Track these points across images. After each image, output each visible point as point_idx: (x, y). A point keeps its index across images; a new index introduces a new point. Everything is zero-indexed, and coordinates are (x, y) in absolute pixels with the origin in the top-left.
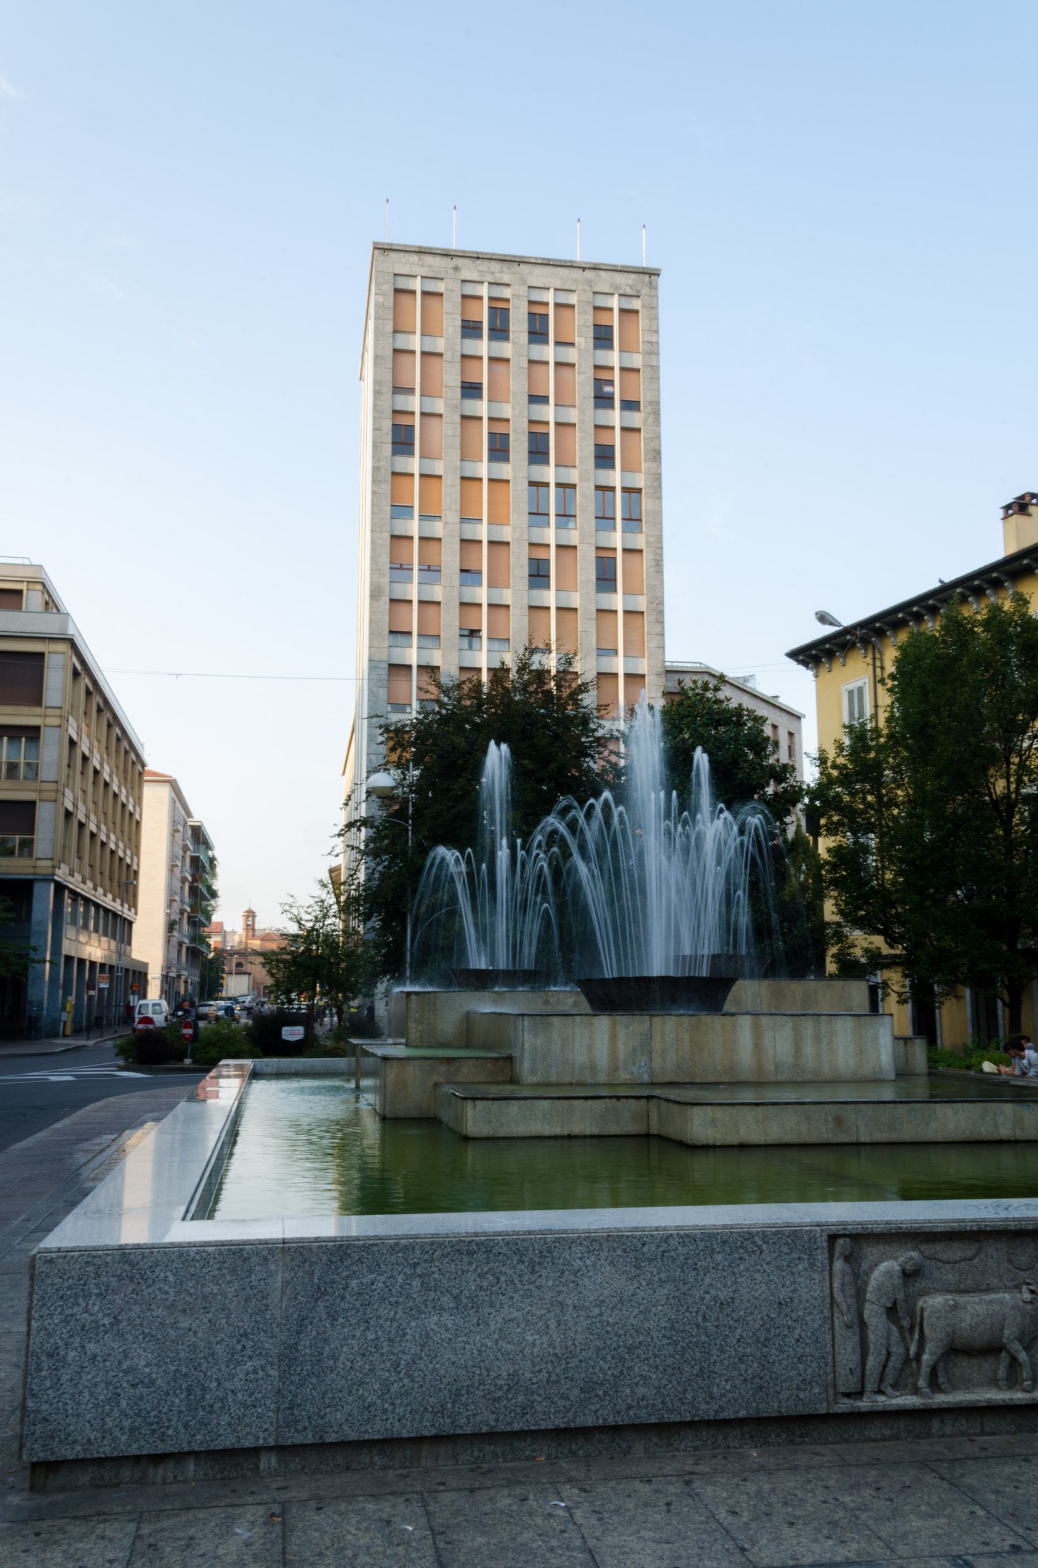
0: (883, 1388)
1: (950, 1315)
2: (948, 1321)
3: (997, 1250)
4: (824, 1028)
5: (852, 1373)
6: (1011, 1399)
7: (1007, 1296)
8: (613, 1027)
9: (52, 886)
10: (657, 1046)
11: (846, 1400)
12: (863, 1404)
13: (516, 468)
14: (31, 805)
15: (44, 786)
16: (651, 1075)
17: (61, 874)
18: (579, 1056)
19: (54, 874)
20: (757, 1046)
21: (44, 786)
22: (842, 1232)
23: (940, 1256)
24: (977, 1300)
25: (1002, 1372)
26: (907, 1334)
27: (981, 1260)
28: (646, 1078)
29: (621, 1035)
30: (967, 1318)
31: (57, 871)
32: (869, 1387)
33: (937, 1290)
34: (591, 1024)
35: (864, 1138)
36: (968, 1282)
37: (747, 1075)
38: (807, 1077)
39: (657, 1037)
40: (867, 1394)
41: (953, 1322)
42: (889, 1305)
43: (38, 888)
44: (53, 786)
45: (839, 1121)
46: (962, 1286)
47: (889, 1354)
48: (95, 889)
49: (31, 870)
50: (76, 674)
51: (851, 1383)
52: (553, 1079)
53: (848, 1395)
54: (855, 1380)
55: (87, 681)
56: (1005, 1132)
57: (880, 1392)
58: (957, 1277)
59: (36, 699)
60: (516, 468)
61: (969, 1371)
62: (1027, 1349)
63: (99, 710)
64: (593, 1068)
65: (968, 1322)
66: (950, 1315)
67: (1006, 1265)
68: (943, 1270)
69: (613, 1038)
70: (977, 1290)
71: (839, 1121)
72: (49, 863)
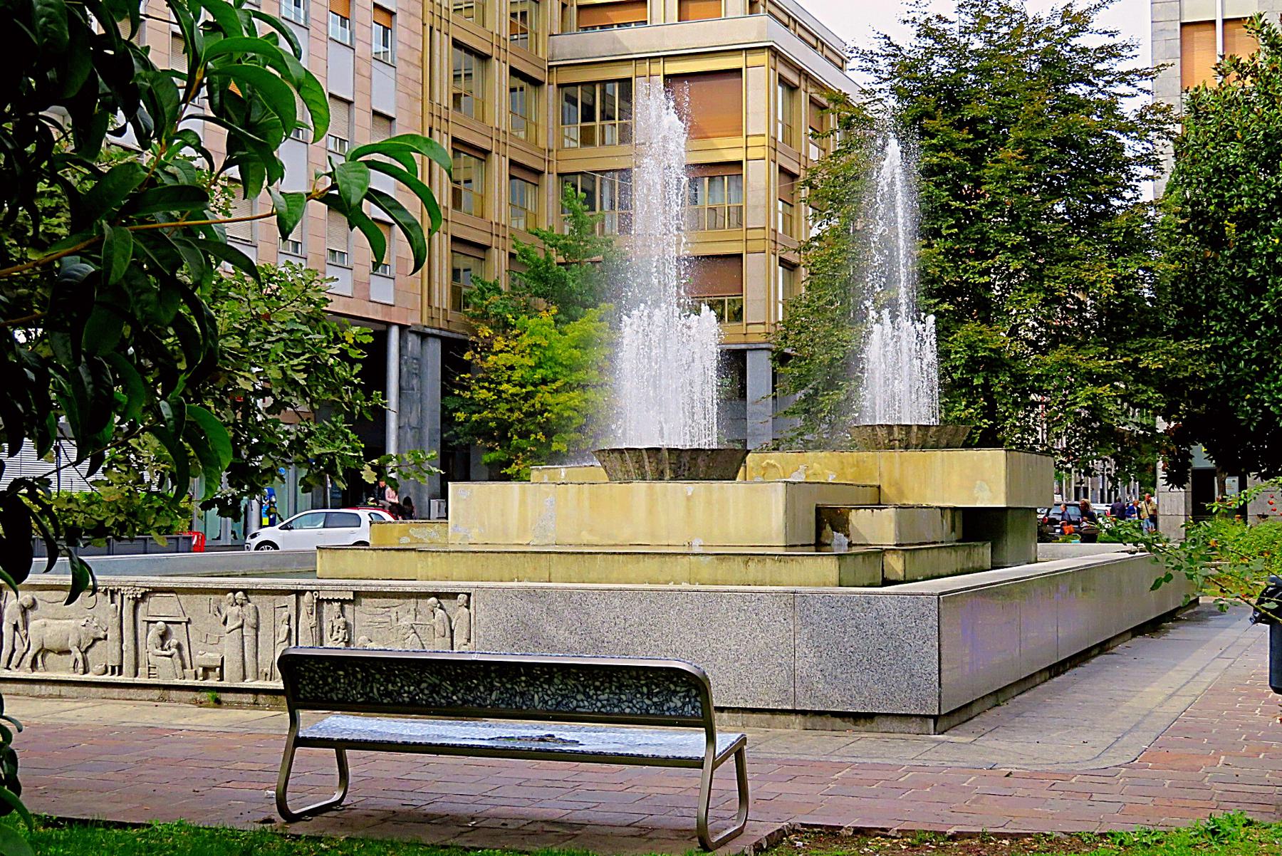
14: (740, 256)
15: (751, 234)
21: (751, 234)
47: (14, 650)
49: (742, 339)
50: (791, 89)
59: (738, 131)
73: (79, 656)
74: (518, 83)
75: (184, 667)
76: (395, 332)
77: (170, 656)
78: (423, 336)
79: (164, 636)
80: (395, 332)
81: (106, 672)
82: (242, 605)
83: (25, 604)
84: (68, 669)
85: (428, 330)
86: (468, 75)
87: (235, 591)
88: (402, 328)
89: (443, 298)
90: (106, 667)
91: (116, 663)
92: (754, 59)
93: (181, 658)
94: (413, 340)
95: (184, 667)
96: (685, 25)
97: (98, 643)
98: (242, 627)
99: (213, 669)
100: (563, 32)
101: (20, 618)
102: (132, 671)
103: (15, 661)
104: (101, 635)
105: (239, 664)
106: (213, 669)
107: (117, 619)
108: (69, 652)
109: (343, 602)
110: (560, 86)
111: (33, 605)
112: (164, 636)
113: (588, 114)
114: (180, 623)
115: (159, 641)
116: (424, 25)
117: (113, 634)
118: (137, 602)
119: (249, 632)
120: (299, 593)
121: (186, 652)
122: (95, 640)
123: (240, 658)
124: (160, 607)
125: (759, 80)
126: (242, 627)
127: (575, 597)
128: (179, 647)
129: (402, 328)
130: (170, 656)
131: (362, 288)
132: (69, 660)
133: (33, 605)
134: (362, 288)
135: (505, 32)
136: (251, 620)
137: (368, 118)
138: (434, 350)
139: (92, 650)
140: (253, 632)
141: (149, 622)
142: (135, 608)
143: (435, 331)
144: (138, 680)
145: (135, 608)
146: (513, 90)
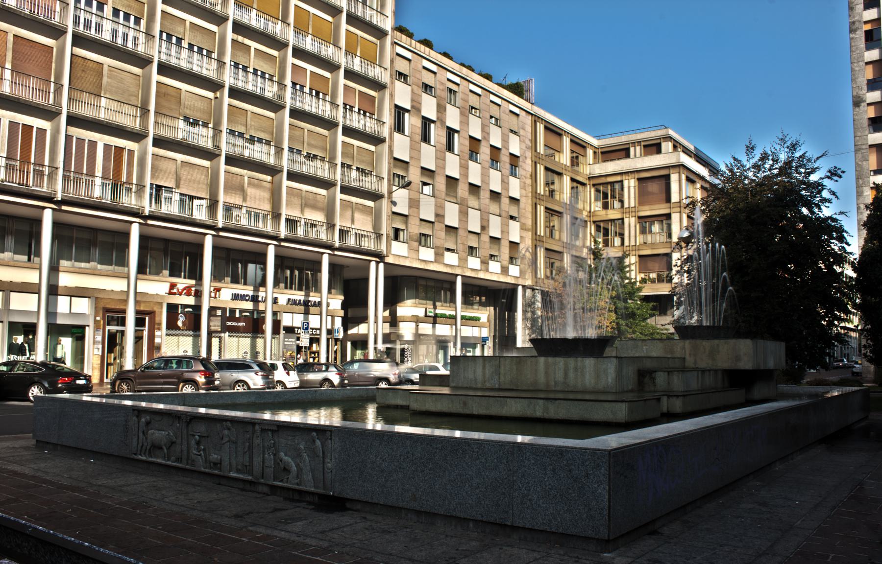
4: (579, 364)
10: (502, 371)
12: (136, 457)
16: (499, 385)
18: (471, 376)
20: (546, 373)
28: (497, 386)
35: (475, 412)
37: (542, 387)
38: (570, 389)
39: (502, 368)
45: (465, 404)
52: (460, 385)
56: (539, 413)
64: (476, 380)
71: (465, 404)
74: (575, 184)
76: (520, 288)
80: (520, 289)
88: (524, 286)
89: (541, 273)
94: (529, 292)
109: (272, 431)
127: (386, 438)
129: (524, 286)
135: (569, 164)
137: (507, 200)
142: (187, 426)
144: (188, 467)
145: (187, 426)
146: (572, 188)
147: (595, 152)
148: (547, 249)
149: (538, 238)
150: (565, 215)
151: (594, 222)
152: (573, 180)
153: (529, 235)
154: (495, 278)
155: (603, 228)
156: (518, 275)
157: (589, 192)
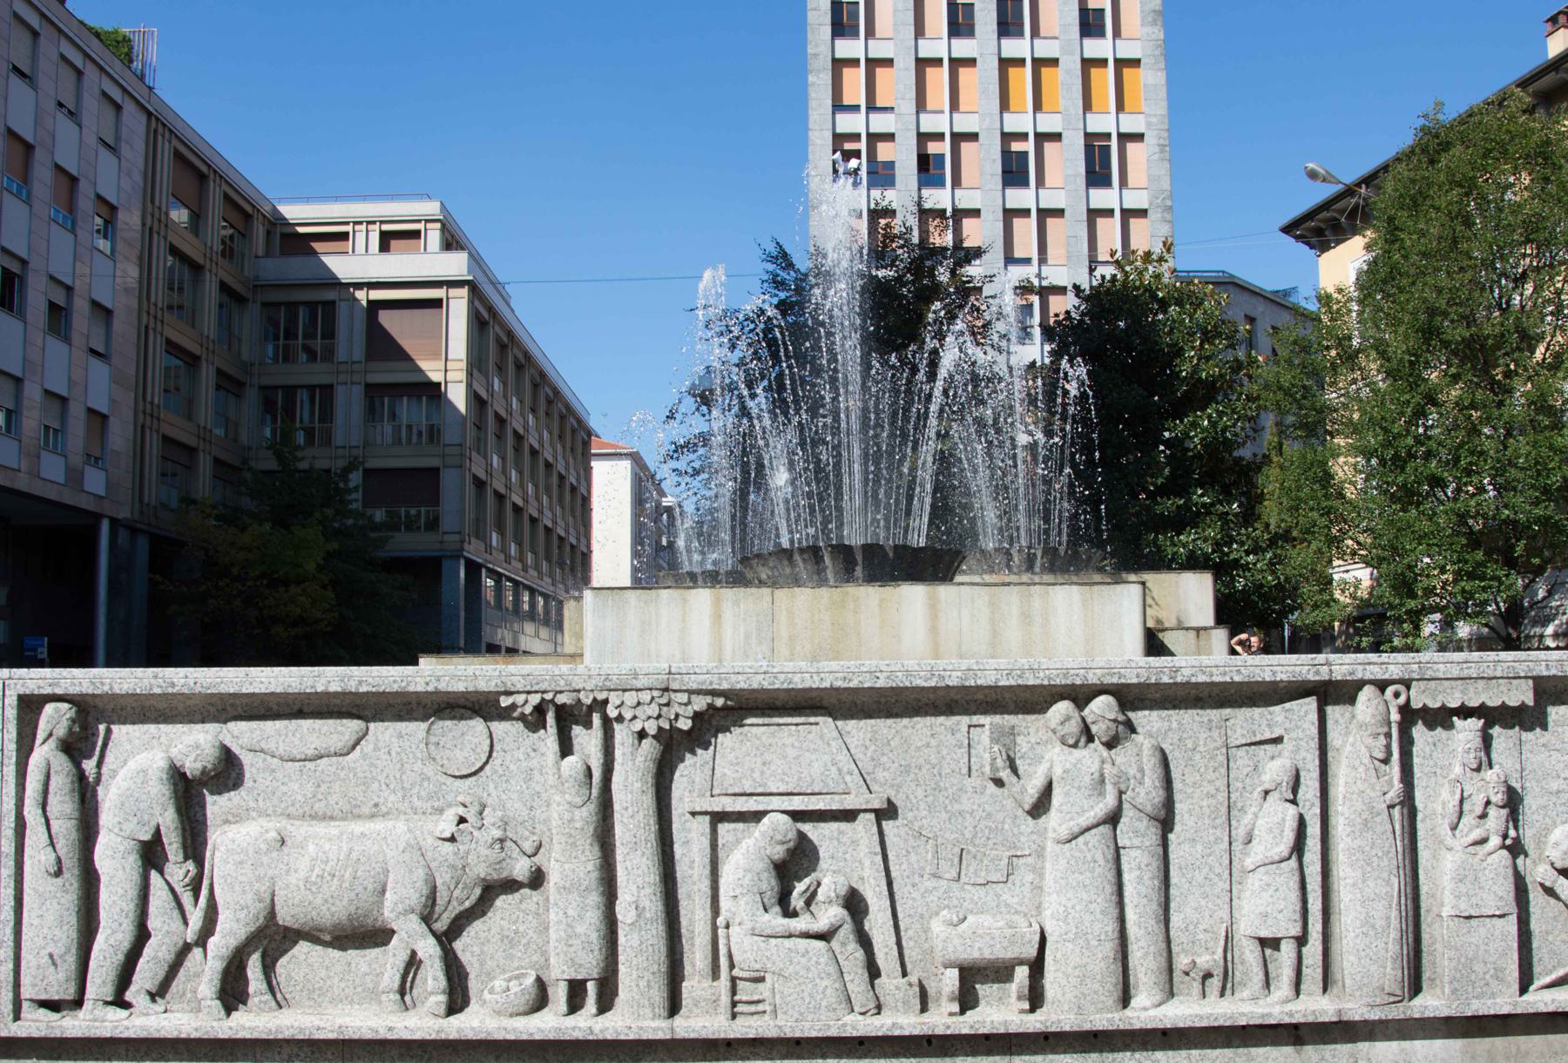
0: (129, 996)
1: (265, 860)
2: (261, 871)
3: (400, 736)
5: (55, 964)
6: (390, 1029)
7: (401, 826)
8: (717, 602)
9: (462, 562)
11: (43, 1013)
12: (73, 1025)
13: (983, 44)
14: (435, 471)
15: (448, 450)
17: (474, 550)
19: (462, 549)
21: (448, 450)
22: (48, 691)
23: (272, 746)
24: (335, 832)
25: (391, 978)
26: (187, 899)
27: (364, 756)
29: (728, 612)
30: (303, 865)
31: (466, 546)
32: (91, 992)
33: (264, 814)
34: (685, 601)
36: (332, 800)
39: (783, 617)
40: (88, 1005)
41: (270, 873)
42: (147, 837)
43: (446, 565)
44: (457, 450)
46: (319, 807)
48: (525, 569)
51: (59, 985)
53: (53, 1006)
54: (62, 976)
55: (497, 328)
57: (120, 1002)
58: (310, 788)
60: (983, 44)
61: (323, 973)
62: (446, 939)
63: (519, 367)
65: (302, 874)
66: (265, 860)
67: (418, 766)
68: (279, 775)
69: (717, 617)
70: (353, 814)
72: (456, 537)
73: (428, 949)
75: (873, 972)
76: (105, 527)
77: (824, 936)
78: (134, 531)
79: (794, 864)
80: (105, 527)
81: (540, 1000)
82: (1110, 745)
83: (192, 767)
84: (373, 995)
85: (138, 526)
86: (181, 289)
87: (1081, 695)
88: (114, 522)
90: (541, 986)
91: (589, 965)
92: (453, 292)
93: (865, 941)
94: (123, 534)
95: (873, 972)
96: (385, 257)
97: (502, 902)
98: (1113, 819)
99: (1000, 972)
100: (268, 254)
101: (168, 819)
102: (659, 994)
103: (147, 972)
104: (520, 868)
105: (1109, 948)
106: (1000, 972)
107: (586, 815)
108: (378, 936)
109: (1494, 716)
110: (265, 305)
111: (227, 773)
112: (794, 864)
113: (290, 334)
114: (849, 816)
115: (769, 883)
116: (144, 225)
117: (570, 865)
118: (672, 748)
119: (1136, 835)
120: (1332, 693)
121: (878, 923)
122: (493, 890)
123: (1111, 927)
124: (746, 759)
125: (459, 307)
126: (1113, 819)
128: (854, 904)
129: (114, 522)
130: (824, 936)
131: (75, 478)
132: (389, 960)
133: (228, 771)
134: (75, 478)
135: (218, 247)
136: (1147, 793)
138: (143, 544)
139: (477, 926)
140: (1152, 835)
141: (718, 818)
143: (145, 527)
146: (221, 306)
147: (268, 232)
148: (167, 440)
149: (148, 411)
150: (204, 365)
151: (261, 387)
152: (224, 287)
153: (128, 399)
154: (51, 494)
155: (278, 402)
156: (102, 493)
157: (249, 322)
